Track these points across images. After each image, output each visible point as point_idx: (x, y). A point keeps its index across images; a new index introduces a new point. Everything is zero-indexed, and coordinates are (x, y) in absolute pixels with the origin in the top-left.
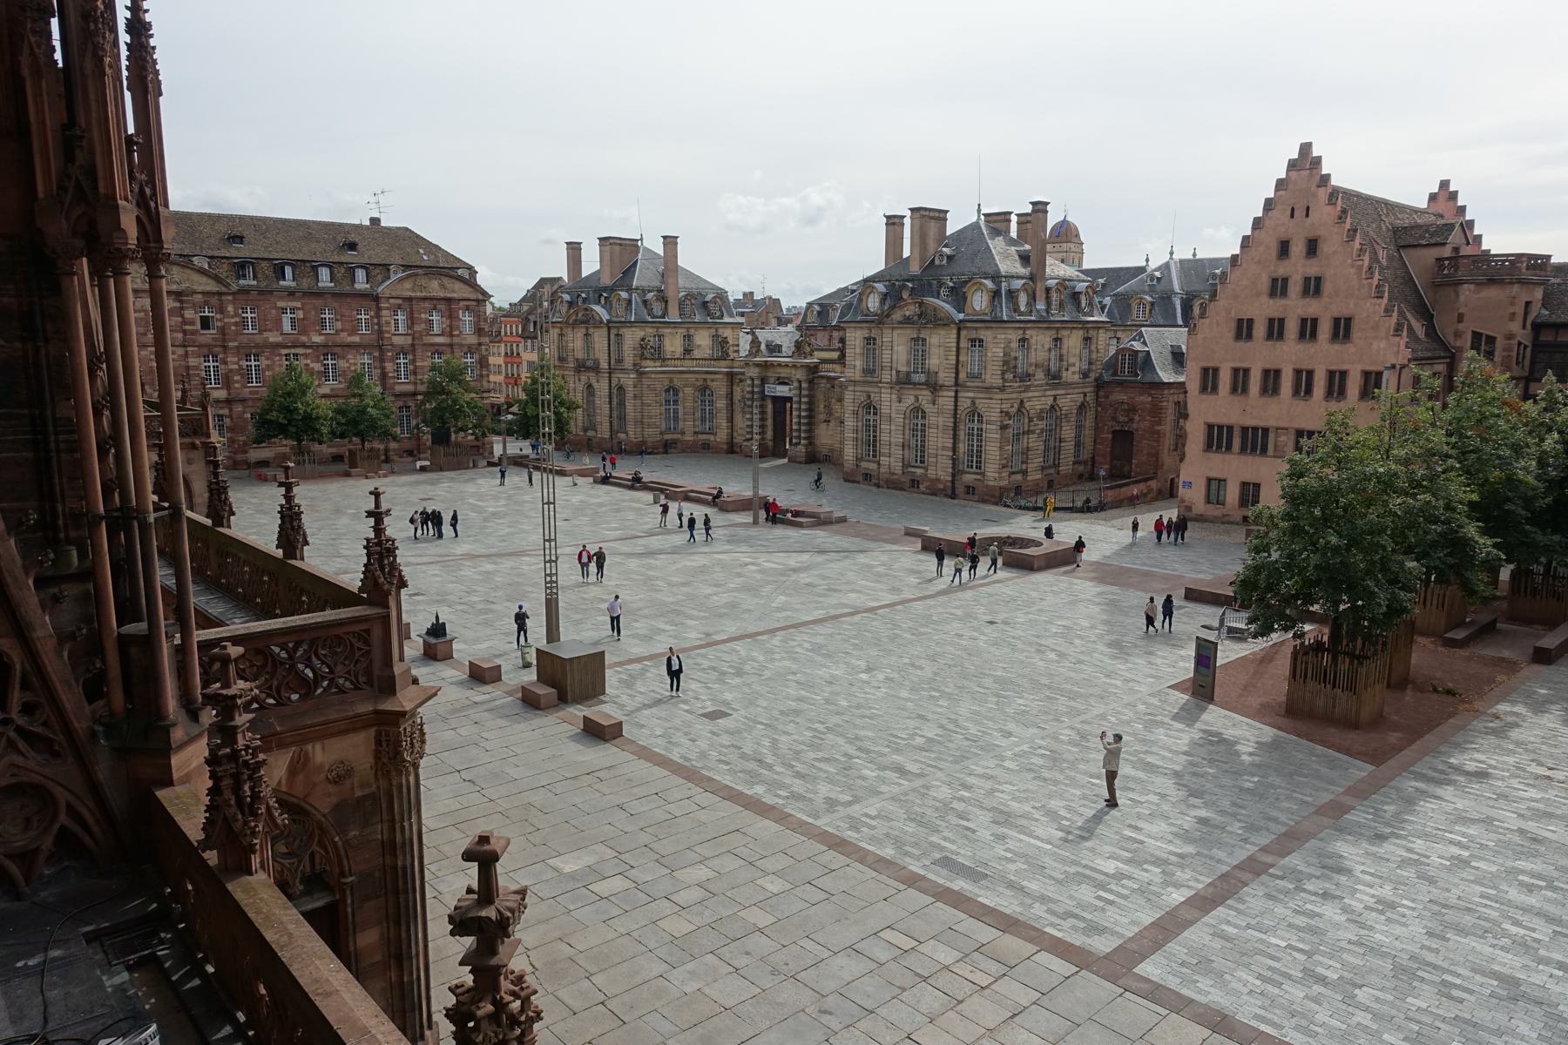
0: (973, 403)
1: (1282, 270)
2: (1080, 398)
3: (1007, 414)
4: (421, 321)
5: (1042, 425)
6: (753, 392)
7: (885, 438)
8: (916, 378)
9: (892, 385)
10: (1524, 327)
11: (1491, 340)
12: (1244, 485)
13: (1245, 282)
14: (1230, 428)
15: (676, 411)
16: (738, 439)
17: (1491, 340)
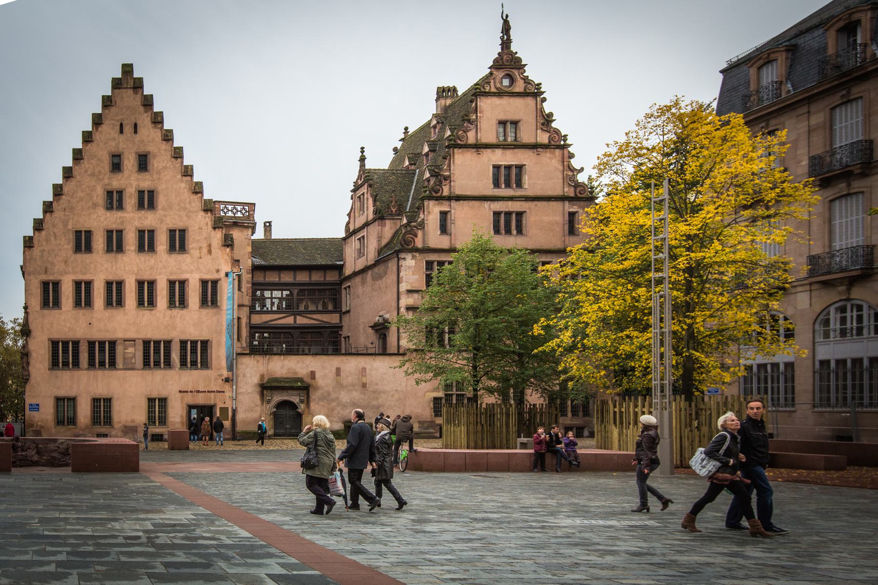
1: (116, 182)
12: (96, 401)
13: (80, 194)
14: (76, 343)
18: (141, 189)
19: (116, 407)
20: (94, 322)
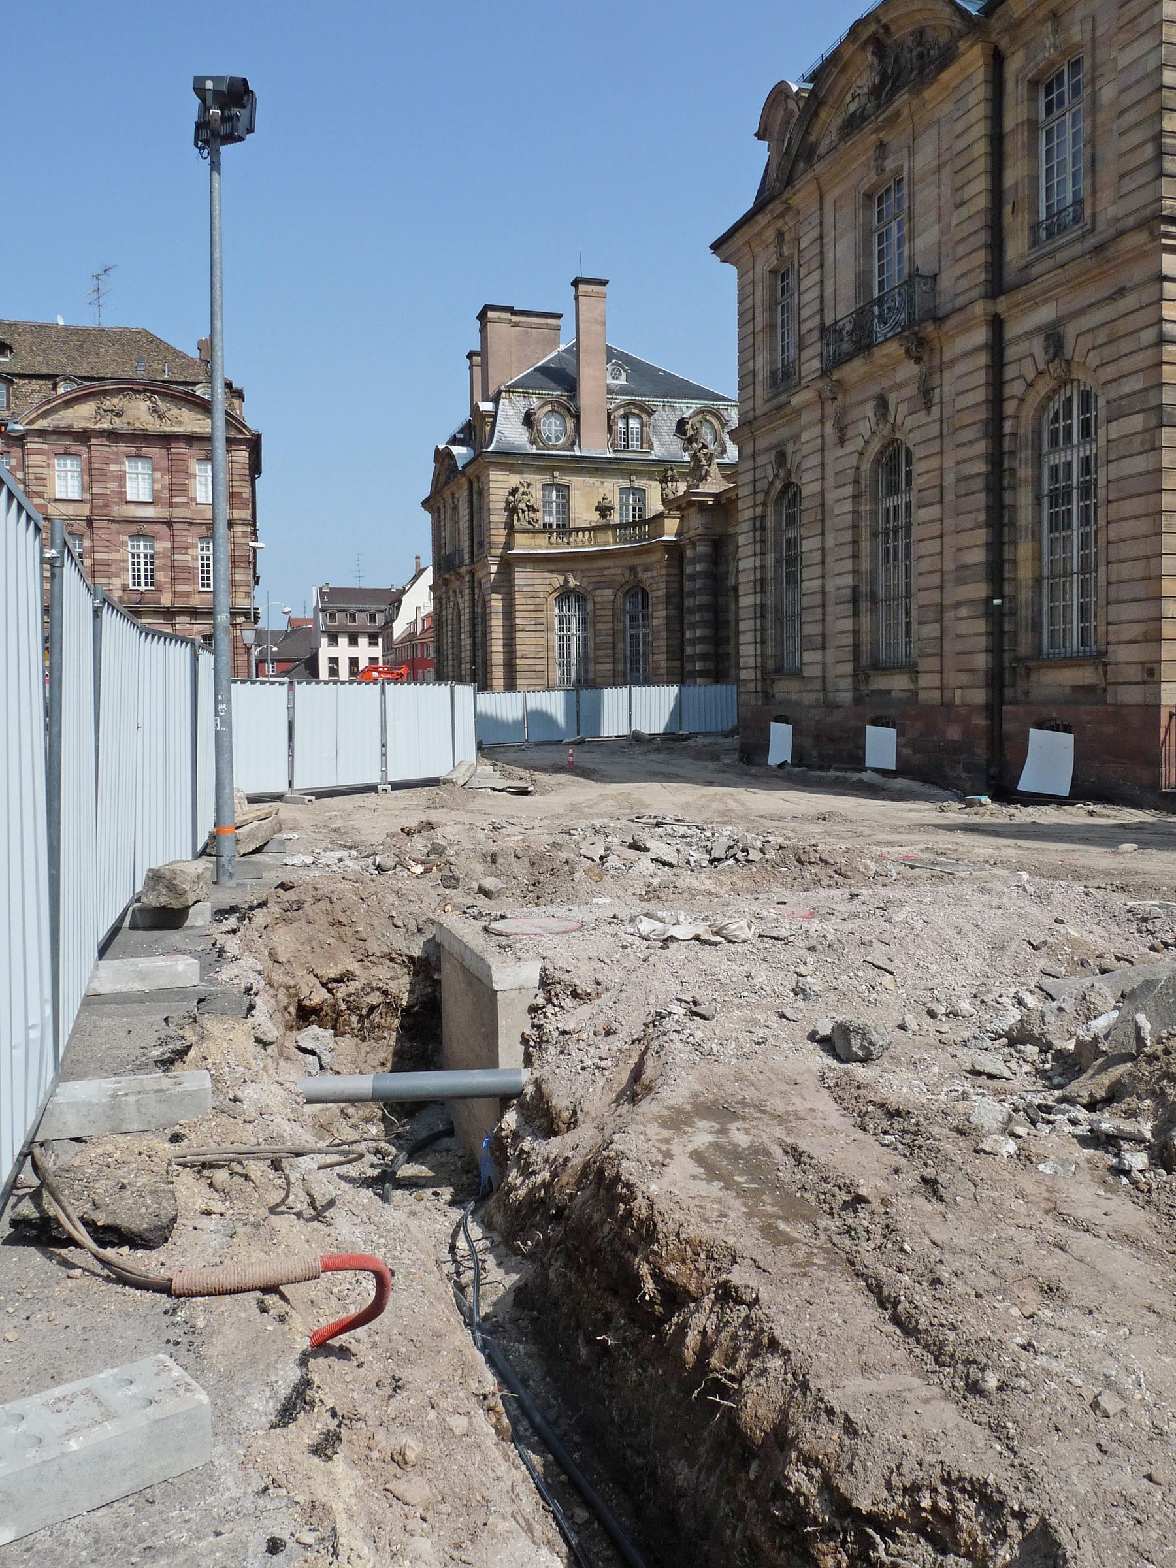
4: (105, 476)
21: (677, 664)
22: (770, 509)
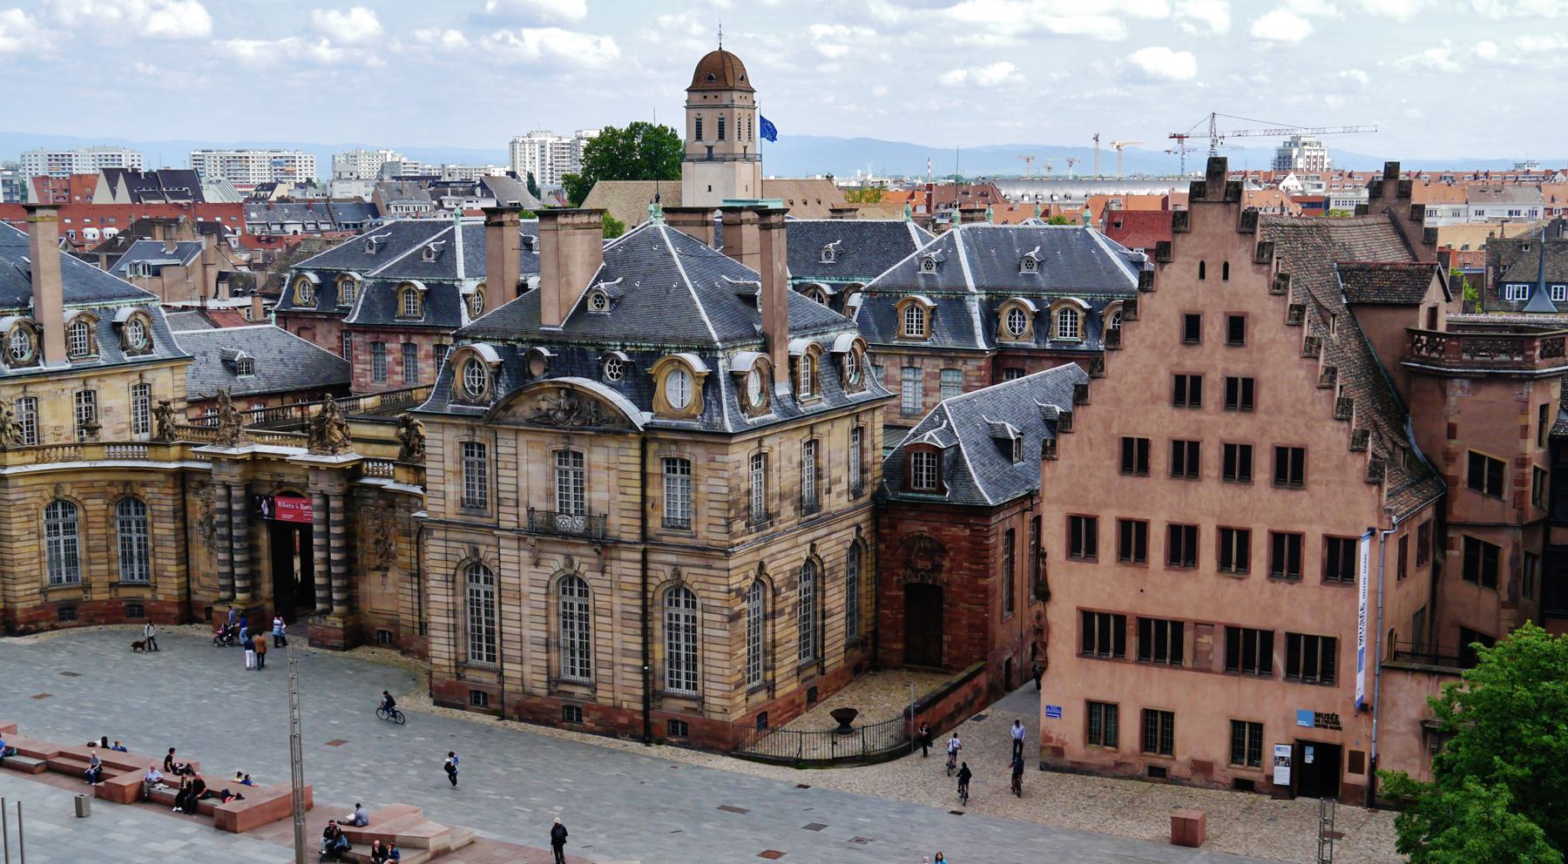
0: (677, 573)
1: (1191, 361)
2: (850, 535)
3: (739, 591)
5: (793, 596)
6: (229, 511)
7: (510, 628)
8: (564, 523)
9: (520, 535)
10: (1540, 444)
11: (1497, 466)
12: (1149, 716)
13: (1132, 378)
14: (1121, 619)
15: (71, 546)
16: (202, 596)
17: (1497, 466)
18: (1232, 375)
19: (1181, 729)
20: (1147, 588)
21: (183, 567)
22: (460, 573)
